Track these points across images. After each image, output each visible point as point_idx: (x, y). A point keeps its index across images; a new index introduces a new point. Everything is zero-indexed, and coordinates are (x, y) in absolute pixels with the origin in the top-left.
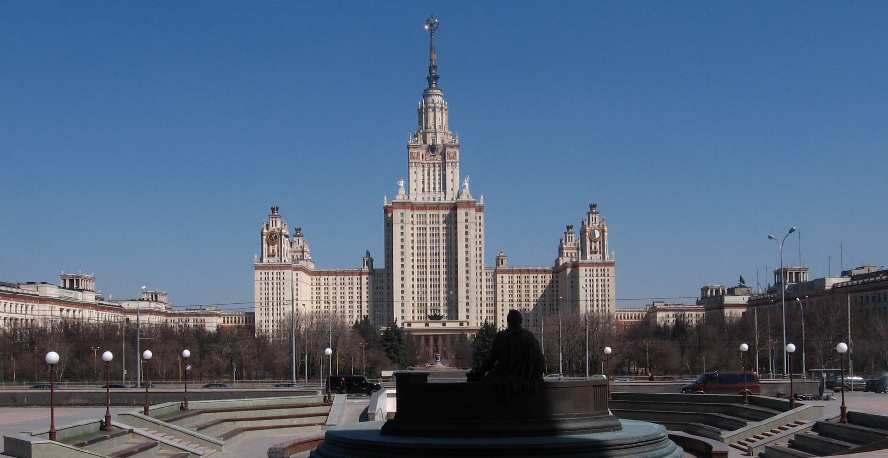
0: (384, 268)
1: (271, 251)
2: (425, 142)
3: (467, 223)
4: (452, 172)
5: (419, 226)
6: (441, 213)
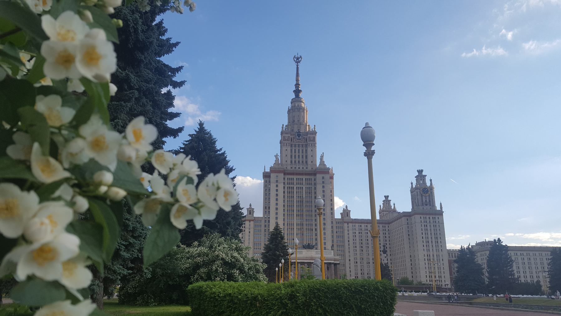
2: (292, 130)
3: (323, 185)
4: (312, 150)
5: (289, 186)
6: (304, 177)
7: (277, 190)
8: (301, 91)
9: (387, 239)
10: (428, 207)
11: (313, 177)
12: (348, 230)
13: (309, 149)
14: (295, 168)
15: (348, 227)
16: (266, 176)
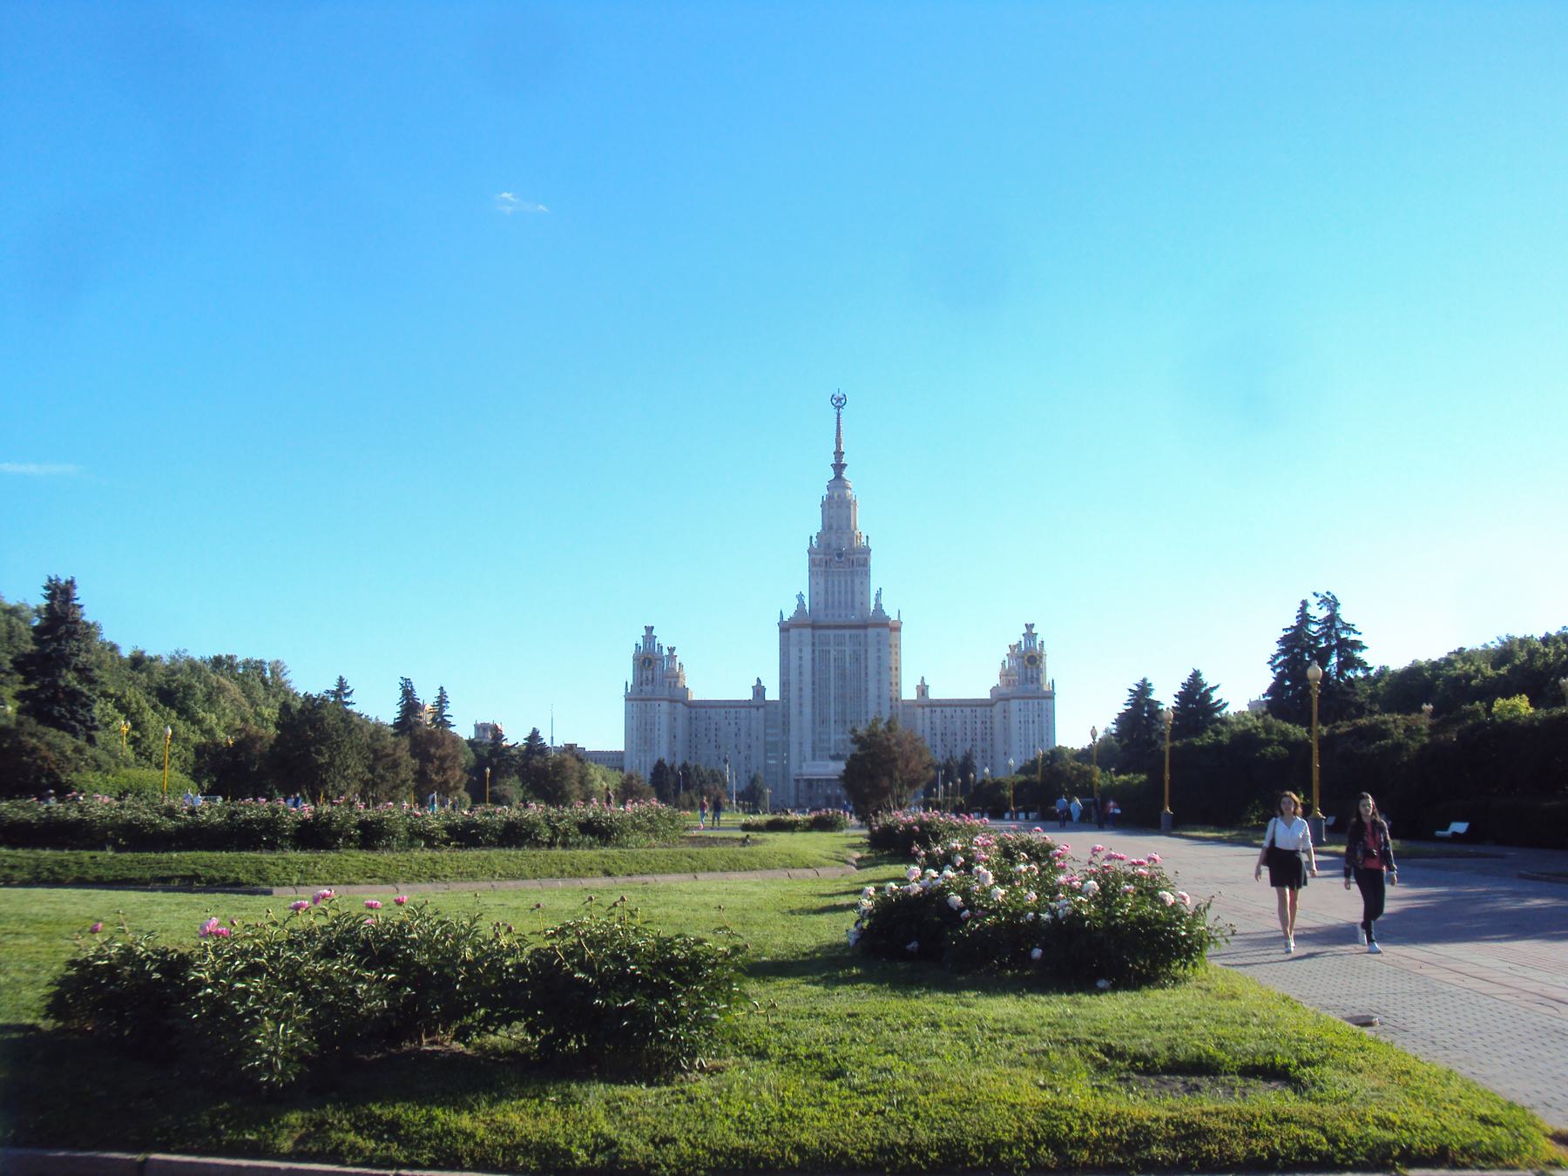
0: (778, 699)
1: (644, 676)
6: (847, 632)
7: (801, 658)
8: (844, 466)
9: (988, 731)
10: (1034, 686)
11: (861, 632)
12: (923, 719)
13: (857, 581)
14: (833, 615)
15: (923, 713)
16: (785, 628)
